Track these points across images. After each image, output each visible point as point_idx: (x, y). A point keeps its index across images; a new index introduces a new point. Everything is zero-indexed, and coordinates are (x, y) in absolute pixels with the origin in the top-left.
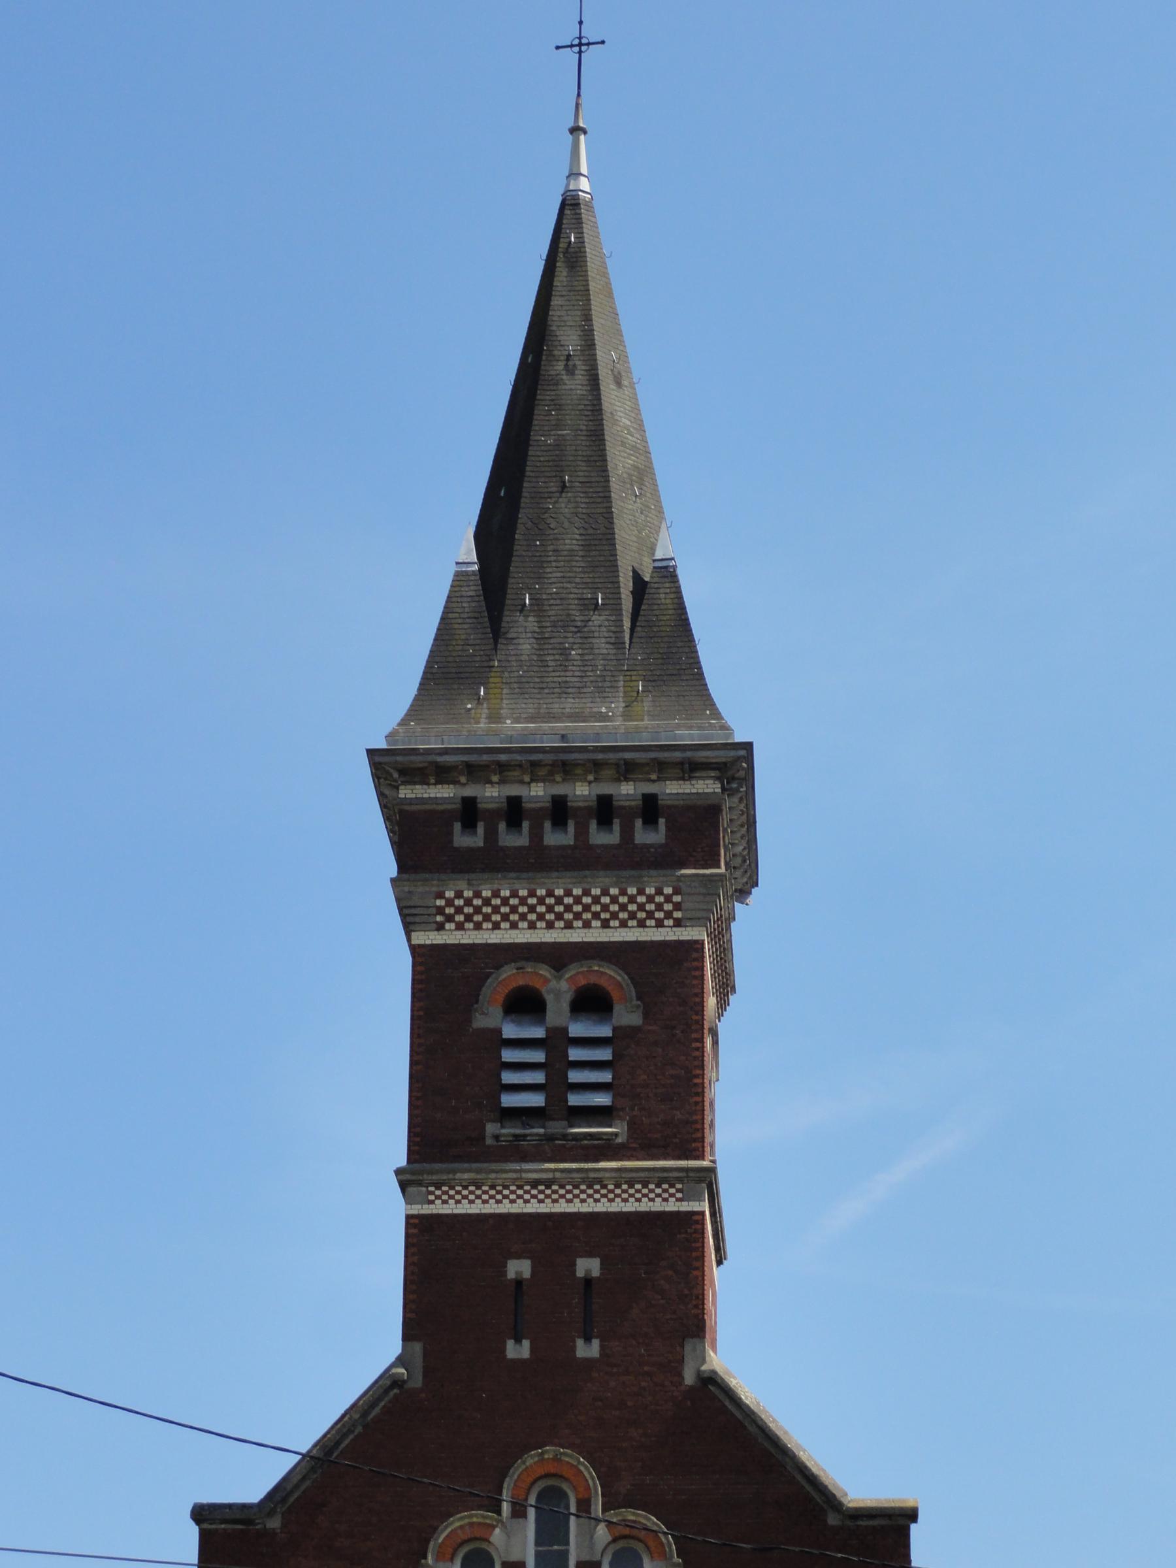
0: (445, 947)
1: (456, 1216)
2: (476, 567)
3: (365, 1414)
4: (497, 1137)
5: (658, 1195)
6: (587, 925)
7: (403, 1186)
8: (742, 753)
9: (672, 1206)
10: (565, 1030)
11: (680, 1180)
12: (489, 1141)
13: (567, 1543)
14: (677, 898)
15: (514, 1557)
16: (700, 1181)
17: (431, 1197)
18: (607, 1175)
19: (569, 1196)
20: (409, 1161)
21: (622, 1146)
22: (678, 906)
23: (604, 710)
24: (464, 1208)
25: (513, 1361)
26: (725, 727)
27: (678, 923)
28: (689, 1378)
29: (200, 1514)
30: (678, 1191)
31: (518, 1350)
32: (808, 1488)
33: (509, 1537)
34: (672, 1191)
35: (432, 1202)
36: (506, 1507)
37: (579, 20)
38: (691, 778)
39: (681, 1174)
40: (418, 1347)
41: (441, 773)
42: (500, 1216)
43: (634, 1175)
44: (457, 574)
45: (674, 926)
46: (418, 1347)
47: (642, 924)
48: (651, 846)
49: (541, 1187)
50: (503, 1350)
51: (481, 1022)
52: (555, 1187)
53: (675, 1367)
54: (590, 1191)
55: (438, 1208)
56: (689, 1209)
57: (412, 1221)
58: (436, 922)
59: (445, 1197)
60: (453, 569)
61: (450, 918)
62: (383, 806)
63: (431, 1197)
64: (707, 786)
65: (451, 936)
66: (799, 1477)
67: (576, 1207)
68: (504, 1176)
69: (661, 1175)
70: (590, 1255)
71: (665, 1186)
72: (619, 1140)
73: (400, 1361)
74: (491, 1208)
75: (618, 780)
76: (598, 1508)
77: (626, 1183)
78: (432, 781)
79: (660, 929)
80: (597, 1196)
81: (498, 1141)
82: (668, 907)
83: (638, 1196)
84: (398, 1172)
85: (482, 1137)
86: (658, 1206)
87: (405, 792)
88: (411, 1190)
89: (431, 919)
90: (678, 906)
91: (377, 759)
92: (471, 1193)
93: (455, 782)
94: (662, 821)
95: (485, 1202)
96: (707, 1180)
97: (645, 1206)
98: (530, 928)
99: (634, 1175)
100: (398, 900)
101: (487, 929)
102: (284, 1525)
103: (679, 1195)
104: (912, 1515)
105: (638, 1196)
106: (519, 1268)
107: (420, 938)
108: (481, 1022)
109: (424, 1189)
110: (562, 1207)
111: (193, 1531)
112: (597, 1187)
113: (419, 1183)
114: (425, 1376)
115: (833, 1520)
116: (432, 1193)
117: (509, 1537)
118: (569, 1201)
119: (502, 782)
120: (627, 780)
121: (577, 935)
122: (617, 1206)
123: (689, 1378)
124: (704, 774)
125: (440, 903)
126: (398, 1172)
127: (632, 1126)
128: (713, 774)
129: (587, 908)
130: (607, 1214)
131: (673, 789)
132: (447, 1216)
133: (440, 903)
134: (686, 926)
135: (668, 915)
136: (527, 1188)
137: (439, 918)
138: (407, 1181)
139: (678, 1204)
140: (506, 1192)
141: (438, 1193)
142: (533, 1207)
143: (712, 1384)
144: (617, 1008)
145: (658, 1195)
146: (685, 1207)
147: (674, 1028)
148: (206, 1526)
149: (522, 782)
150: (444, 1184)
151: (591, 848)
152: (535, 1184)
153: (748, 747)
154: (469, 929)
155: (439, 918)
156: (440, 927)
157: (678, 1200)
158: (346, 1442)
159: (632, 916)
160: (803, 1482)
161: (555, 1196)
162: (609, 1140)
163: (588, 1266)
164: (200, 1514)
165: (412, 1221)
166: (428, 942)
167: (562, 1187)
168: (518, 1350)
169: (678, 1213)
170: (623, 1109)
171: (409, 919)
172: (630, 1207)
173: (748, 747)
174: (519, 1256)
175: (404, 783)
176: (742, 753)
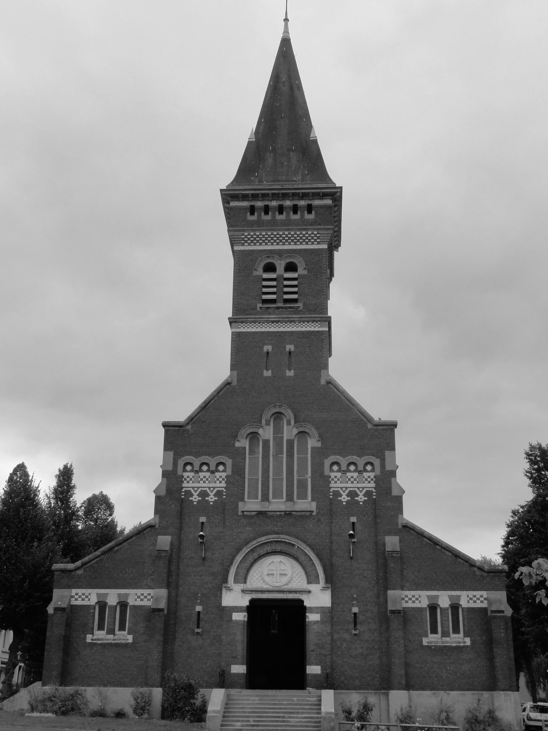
0: (244, 251)
1: (247, 332)
2: (254, 140)
3: (218, 393)
4: (261, 308)
5: (313, 326)
6: (290, 244)
7: (231, 323)
8: (339, 190)
9: (317, 329)
10: (283, 276)
11: (319, 321)
12: (258, 309)
13: (283, 434)
14: (318, 235)
15: (266, 438)
16: (325, 321)
17: (240, 326)
18: (296, 319)
19: (284, 326)
20: (233, 315)
21: (301, 311)
22: (318, 238)
23: (295, 179)
24: (250, 330)
25: (266, 377)
26: (334, 183)
27: (319, 243)
28: (323, 382)
29: (165, 425)
30: (319, 324)
31: (267, 373)
32: (361, 416)
33: (264, 431)
34: (317, 324)
35: (240, 328)
36: (263, 421)
37: (284, 18)
38: (322, 199)
39: (320, 319)
40: (235, 373)
41: (245, 197)
42: (262, 332)
43: (305, 319)
44: (249, 142)
45: (317, 244)
46: (235, 373)
47: (307, 243)
48: (310, 219)
49: (275, 323)
50: (262, 373)
51: (255, 273)
52: (279, 323)
53: (318, 378)
54: (291, 325)
55: (242, 330)
56: (323, 330)
57: (233, 334)
58: (242, 243)
59: (244, 326)
60: (248, 140)
61: (246, 242)
62: (225, 208)
63: (240, 326)
64: (328, 202)
65: (247, 248)
66: (358, 413)
67: (286, 329)
68: (263, 319)
69: (313, 319)
70: (291, 344)
71: (315, 323)
72: (300, 309)
73: (230, 376)
74: (259, 330)
75: (299, 200)
76: (293, 422)
77: (302, 322)
78: (241, 200)
79: (313, 245)
80: (293, 326)
81: (261, 309)
82: (315, 238)
83: (306, 326)
84: (229, 319)
85: (256, 308)
86: (312, 329)
87: (233, 204)
88: (233, 324)
89: (240, 242)
90: (318, 238)
91: (223, 192)
92: (252, 325)
93: (248, 200)
94: (313, 212)
95: (257, 328)
96: (328, 321)
97: (308, 329)
98: (271, 245)
99: (305, 319)
100: (230, 236)
101: (258, 245)
102: (192, 428)
103: (319, 326)
104: (395, 425)
105: (306, 326)
106: (268, 348)
107: (236, 248)
108: (255, 273)
109: (237, 324)
110: (282, 329)
111: (163, 430)
112: (293, 323)
113: (236, 322)
114: (238, 381)
115: (370, 426)
116: (240, 325)
117: (264, 431)
118: (284, 328)
119: (263, 200)
120: (302, 200)
121: (286, 247)
122: (299, 329)
123: (323, 382)
124: (327, 198)
125: (244, 237)
126: (229, 319)
127: (304, 304)
128: (329, 197)
129: (289, 238)
130: (296, 331)
131: (317, 202)
132: (245, 332)
133: (244, 237)
134: (321, 244)
135: (315, 240)
136: (270, 323)
137: (243, 242)
138: (232, 322)
139: (319, 328)
140: (264, 325)
141: (242, 325)
142: (272, 329)
143: (330, 383)
144: (299, 269)
145: (313, 326)
146: (321, 329)
147: (317, 275)
148: (166, 428)
149: (269, 200)
150: (244, 322)
151: (290, 220)
152: (273, 322)
153: (341, 188)
154: (252, 245)
155: (243, 242)
156: (243, 245)
157: (319, 327)
158: (212, 402)
159: (304, 241)
160: (360, 414)
161: (279, 326)
162: (297, 309)
163: (290, 347)
164: (165, 425)
165: (233, 334)
166: (239, 249)
167: (282, 323)
168: (267, 373)
169: (318, 332)
170: (300, 300)
171: (233, 242)
172: (304, 329)
173: (341, 188)
174: (268, 344)
175: (231, 201)
176: (339, 190)
